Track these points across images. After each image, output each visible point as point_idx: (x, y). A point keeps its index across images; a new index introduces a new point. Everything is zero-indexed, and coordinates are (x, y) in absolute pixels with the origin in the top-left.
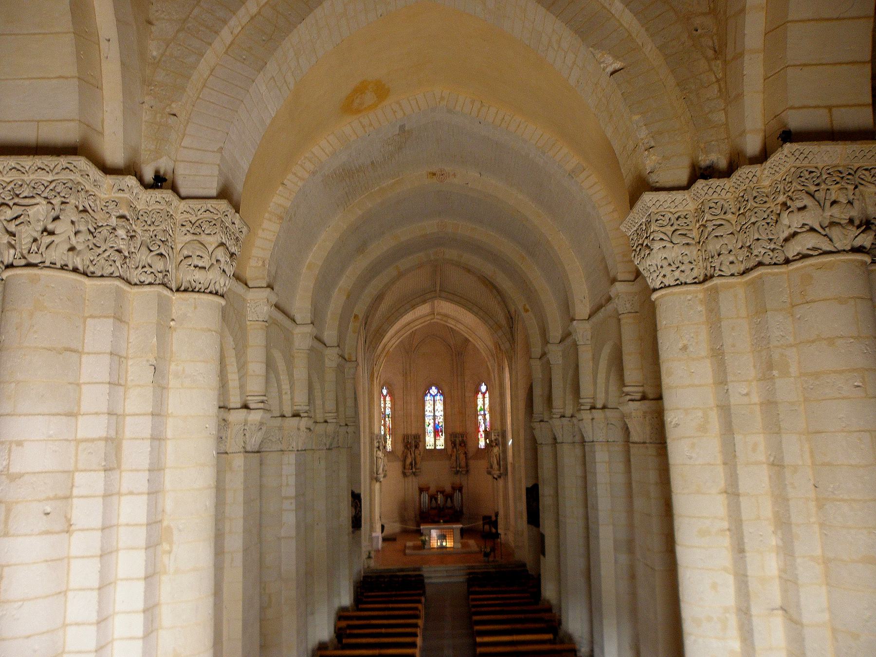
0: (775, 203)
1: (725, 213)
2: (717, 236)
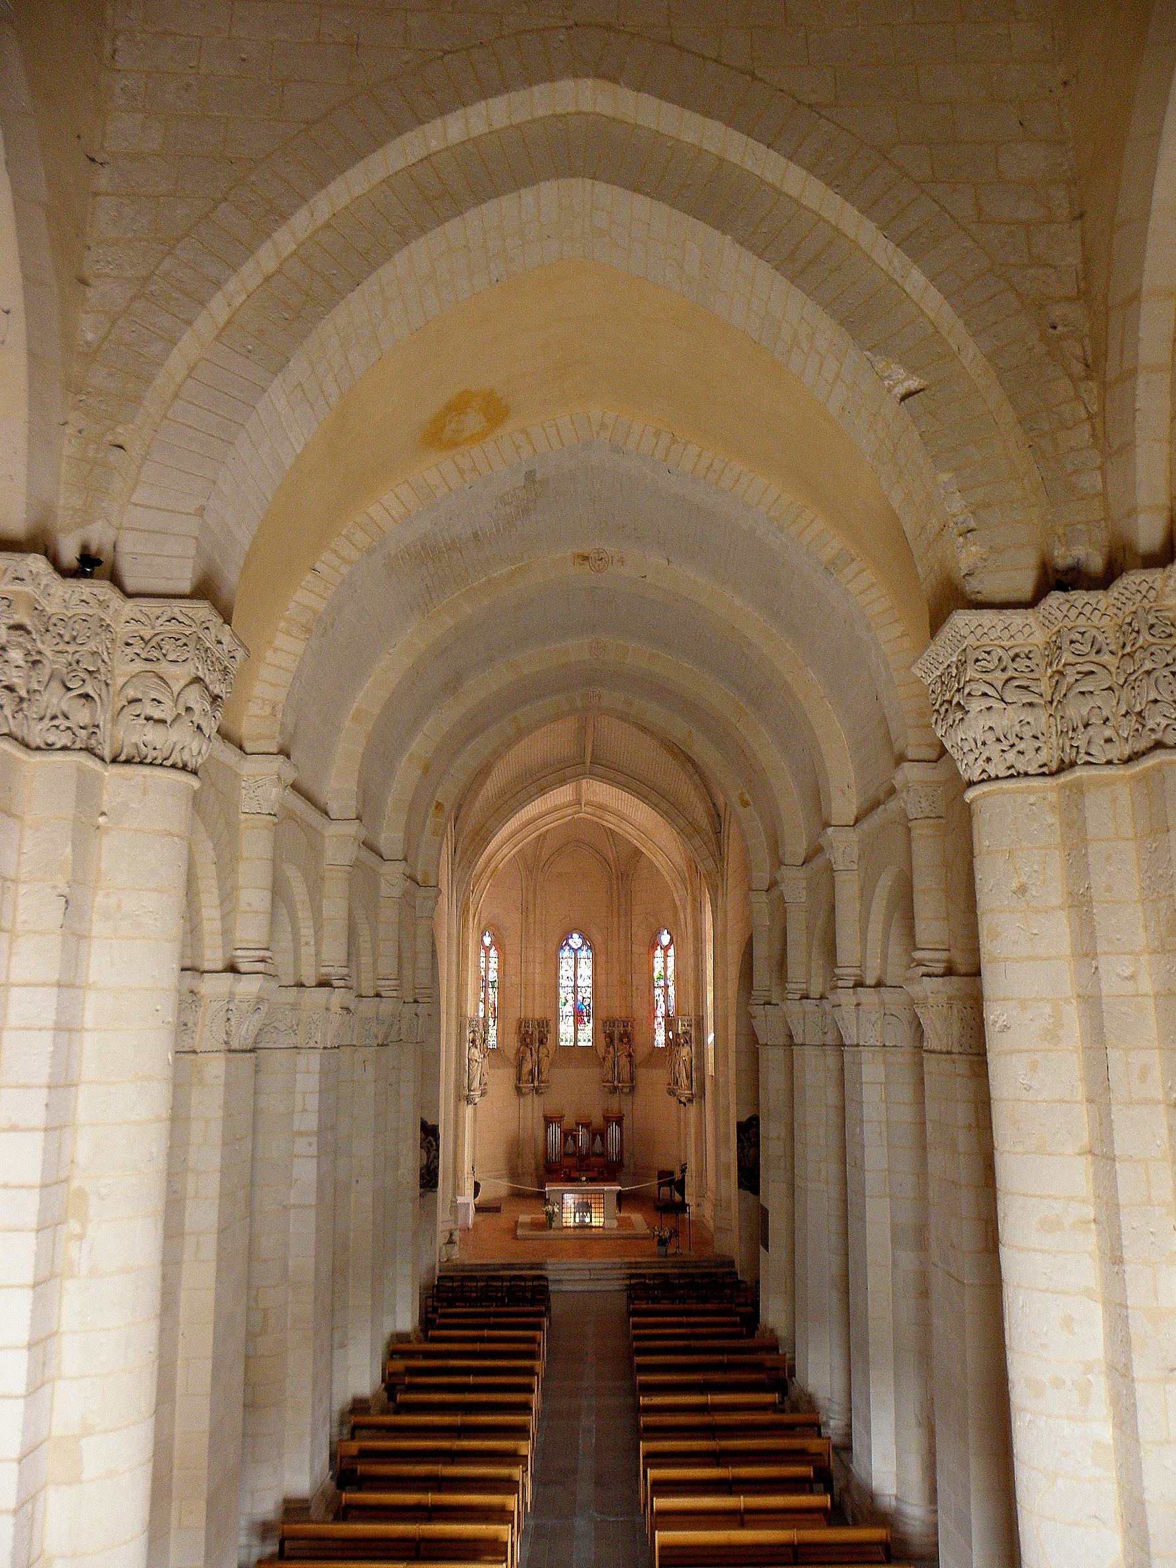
1: (1098, 652)
2: (1083, 693)
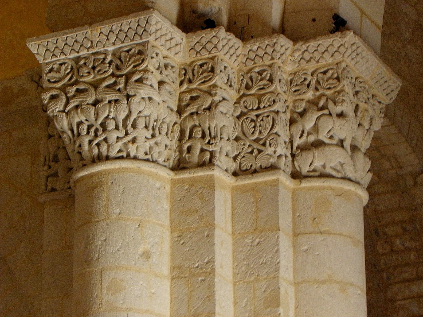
0: (298, 97)
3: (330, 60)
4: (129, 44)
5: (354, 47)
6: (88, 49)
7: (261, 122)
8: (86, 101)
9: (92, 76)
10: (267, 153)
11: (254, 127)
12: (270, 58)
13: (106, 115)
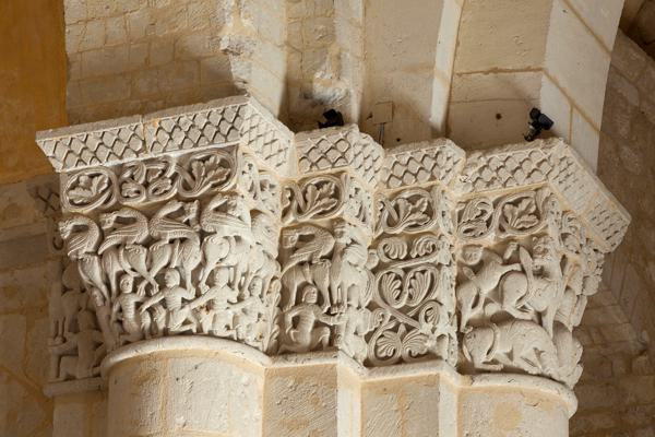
0: (472, 242)
3: (526, 184)
4: (205, 148)
5: (564, 164)
6: (137, 153)
7: (413, 281)
8: (133, 238)
9: (144, 198)
10: (420, 331)
11: (401, 288)
12: (428, 176)
13: (165, 263)
